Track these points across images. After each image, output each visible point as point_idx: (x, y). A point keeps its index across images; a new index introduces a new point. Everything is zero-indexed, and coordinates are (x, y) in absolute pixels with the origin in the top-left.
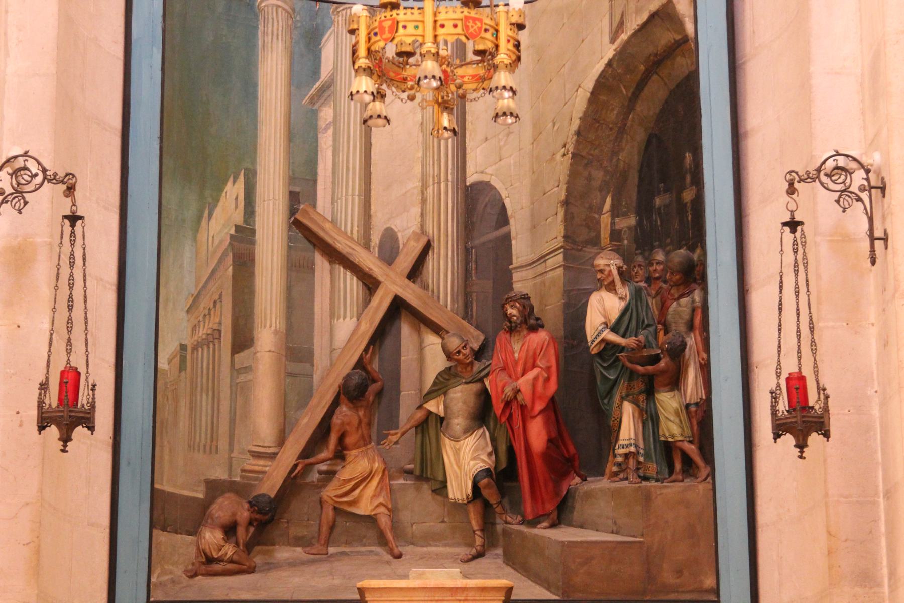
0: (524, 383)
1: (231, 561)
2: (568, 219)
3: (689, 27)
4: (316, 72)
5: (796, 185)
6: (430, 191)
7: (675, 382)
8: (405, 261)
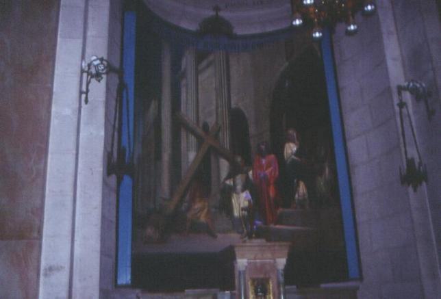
0: (268, 172)
6: (220, 110)
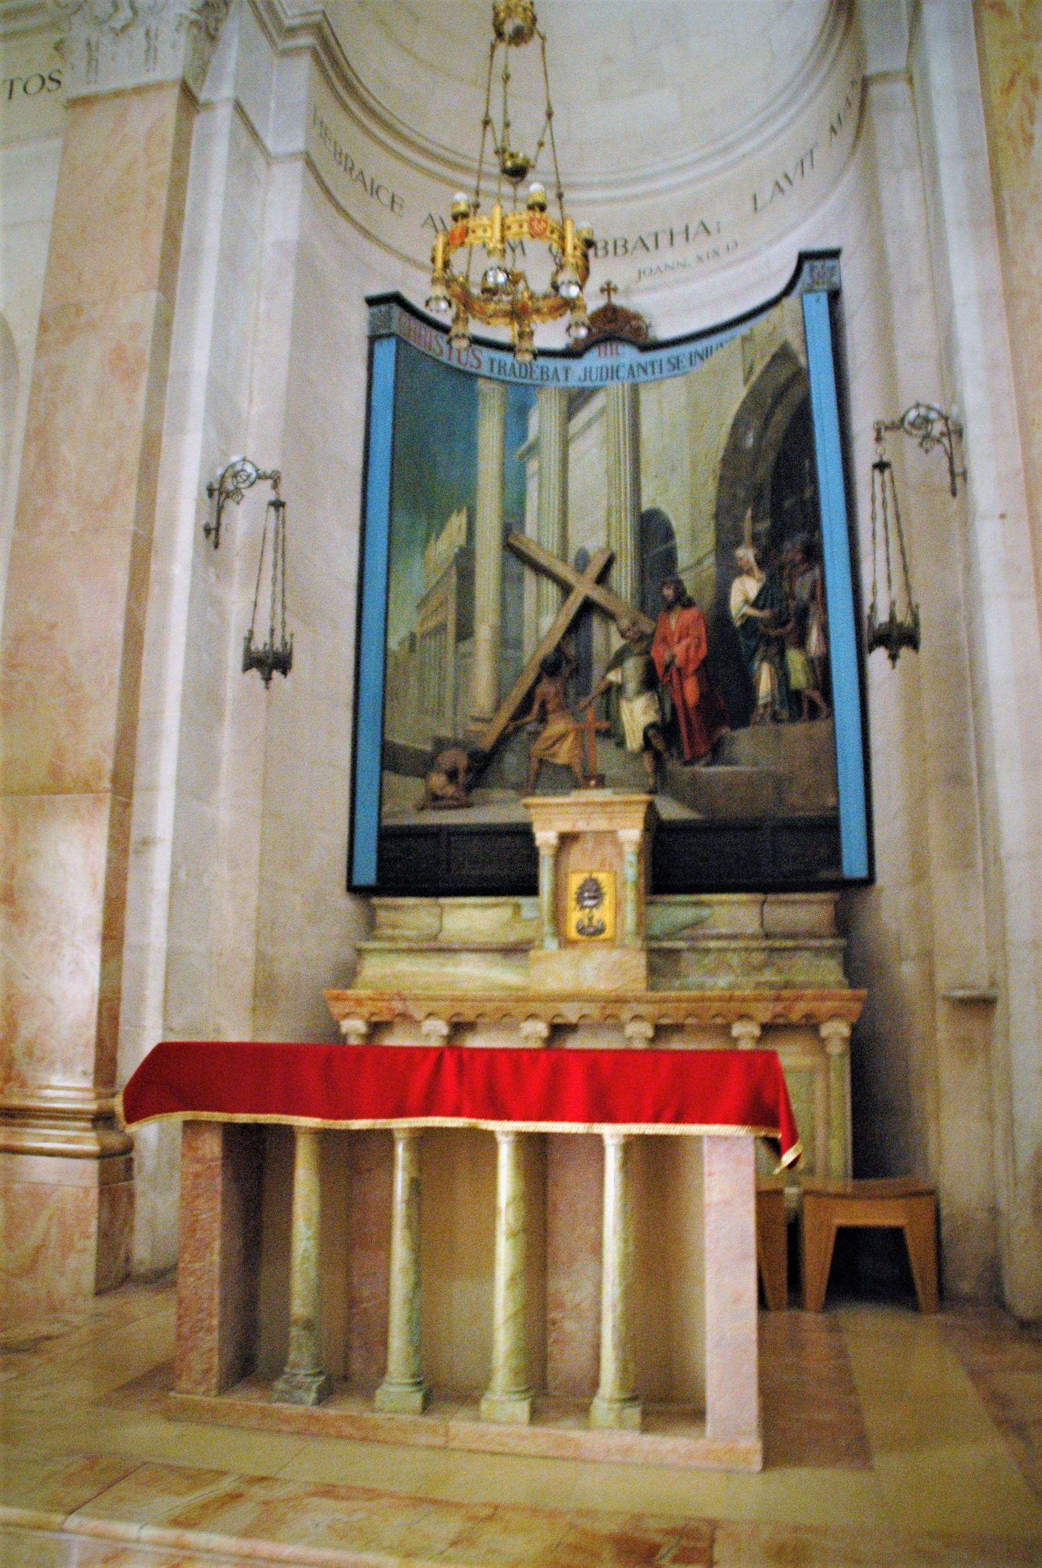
1: (452, 798)
2: (719, 528)
3: (802, 360)
4: (524, 436)
5: (883, 433)
7: (801, 642)
8: (594, 570)
